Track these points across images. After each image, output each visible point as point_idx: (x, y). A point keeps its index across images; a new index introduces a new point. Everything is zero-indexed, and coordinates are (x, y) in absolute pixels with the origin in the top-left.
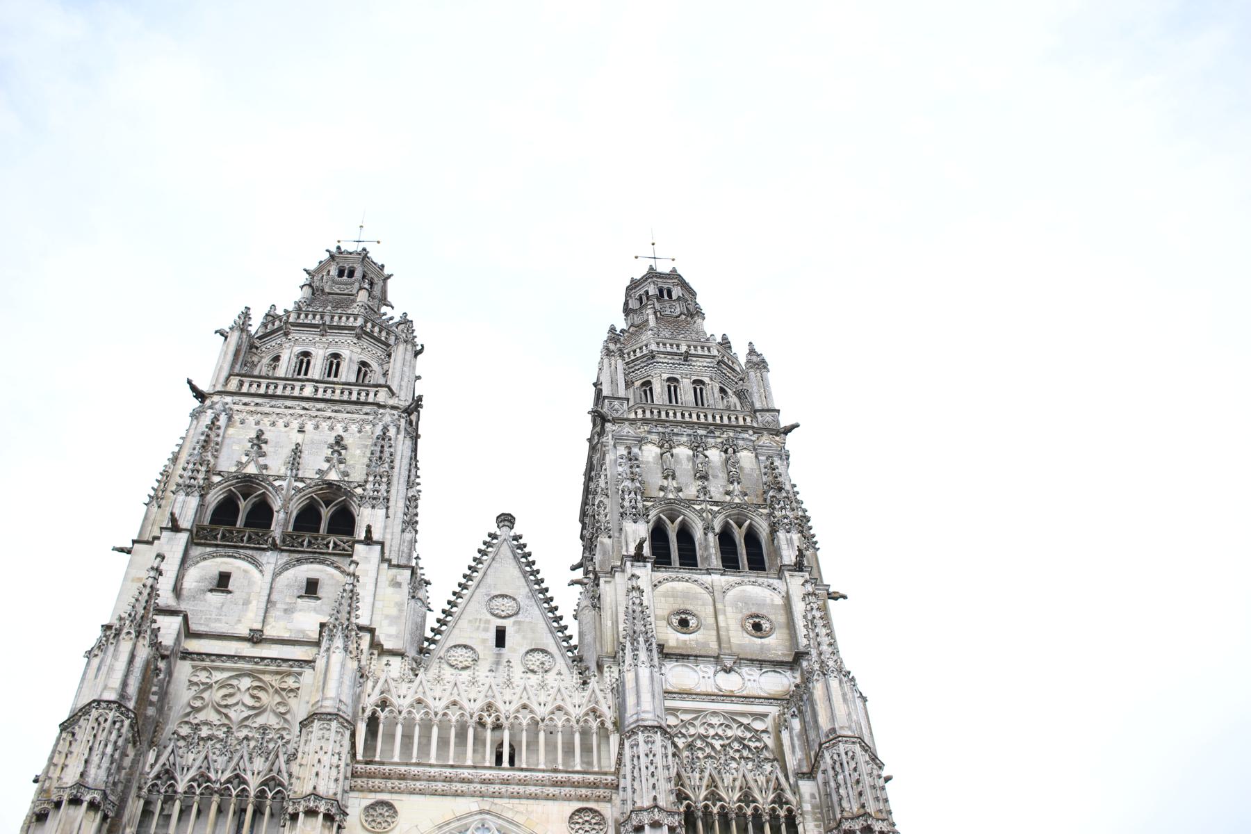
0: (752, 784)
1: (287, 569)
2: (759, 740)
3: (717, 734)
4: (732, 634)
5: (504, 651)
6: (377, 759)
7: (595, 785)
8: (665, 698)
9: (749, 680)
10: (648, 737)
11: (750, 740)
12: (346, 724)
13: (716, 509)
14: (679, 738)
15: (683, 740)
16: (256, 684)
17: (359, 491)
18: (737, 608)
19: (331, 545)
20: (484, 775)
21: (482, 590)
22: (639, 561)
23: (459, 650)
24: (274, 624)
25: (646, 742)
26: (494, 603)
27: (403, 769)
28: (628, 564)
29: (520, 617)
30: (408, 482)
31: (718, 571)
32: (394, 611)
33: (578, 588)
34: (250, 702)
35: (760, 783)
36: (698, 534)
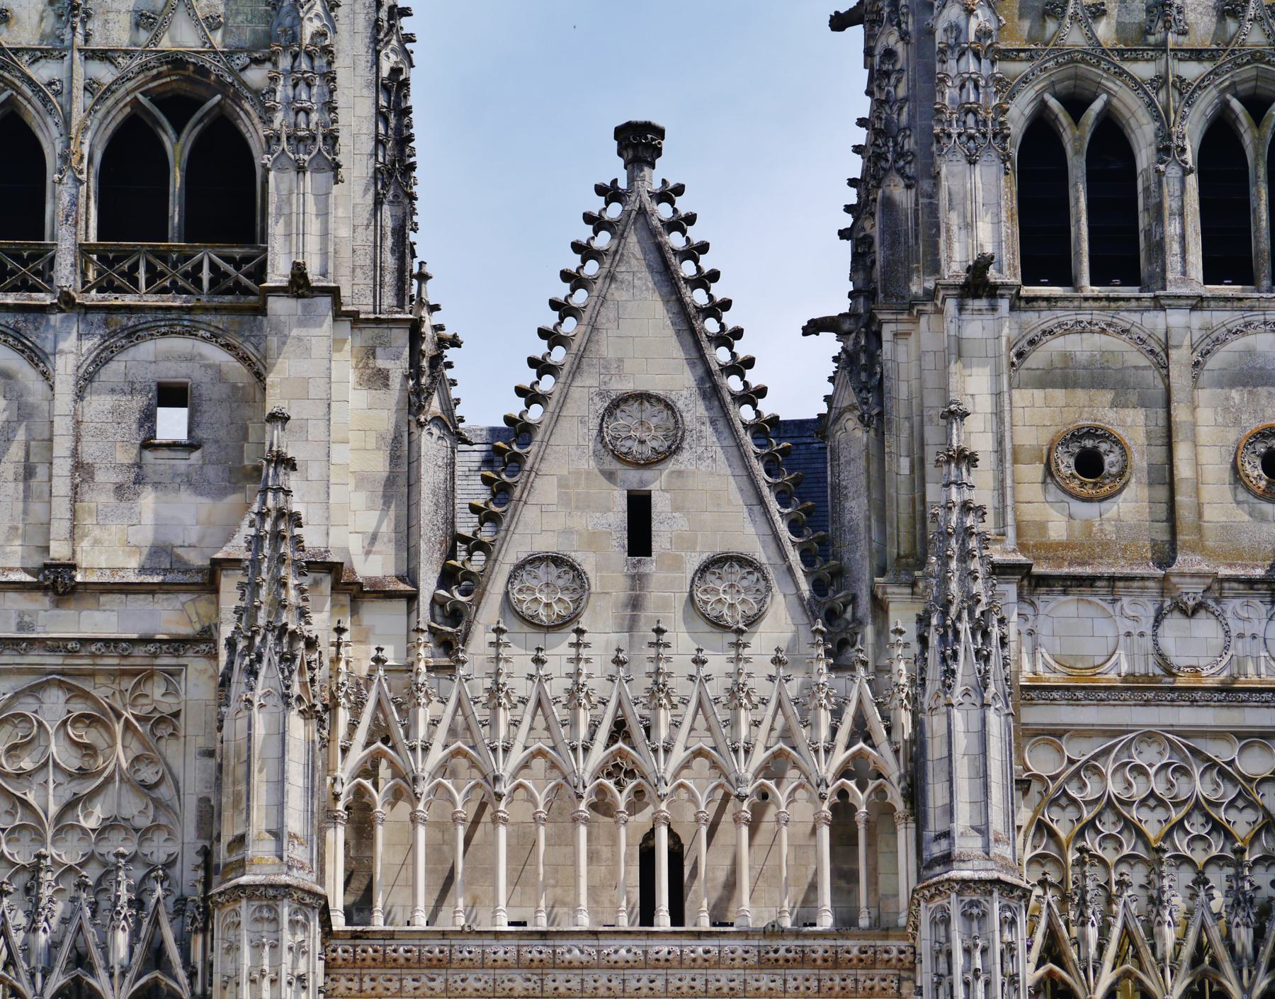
0: (1220, 950)
1: (108, 361)
2: (1252, 805)
3: (1152, 794)
4: (1207, 493)
5: (650, 566)
6: (378, 923)
7: (868, 961)
8: (1030, 702)
9: (1241, 636)
10: (973, 904)
11: (1232, 804)
12: (308, 901)
13: (1191, 70)
14: (1063, 808)
15: (1071, 813)
16: (79, 708)
17: (256, 76)
18: (1226, 410)
19: (206, 275)
20: (616, 952)
21: (588, 381)
22: (977, 296)
23: (541, 571)
24: (96, 532)
25: (967, 916)
26: (626, 420)
27: (435, 947)
28: (951, 305)
29: (685, 456)
30: (377, 26)
31: (1183, 302)
32: (379, 464)
33: (830, 344)
34: (71, 761)
35: (1238, 948)
36: (1144, 157)
